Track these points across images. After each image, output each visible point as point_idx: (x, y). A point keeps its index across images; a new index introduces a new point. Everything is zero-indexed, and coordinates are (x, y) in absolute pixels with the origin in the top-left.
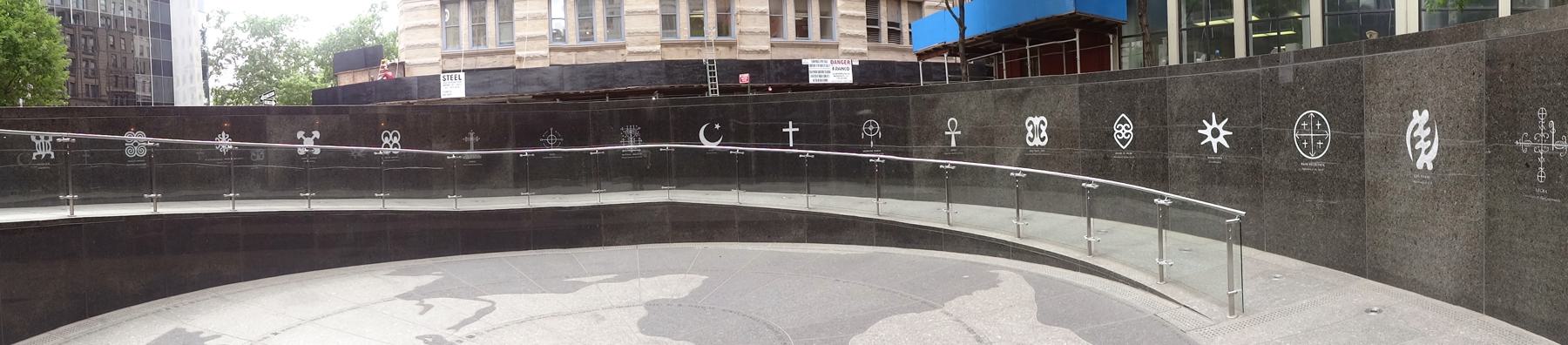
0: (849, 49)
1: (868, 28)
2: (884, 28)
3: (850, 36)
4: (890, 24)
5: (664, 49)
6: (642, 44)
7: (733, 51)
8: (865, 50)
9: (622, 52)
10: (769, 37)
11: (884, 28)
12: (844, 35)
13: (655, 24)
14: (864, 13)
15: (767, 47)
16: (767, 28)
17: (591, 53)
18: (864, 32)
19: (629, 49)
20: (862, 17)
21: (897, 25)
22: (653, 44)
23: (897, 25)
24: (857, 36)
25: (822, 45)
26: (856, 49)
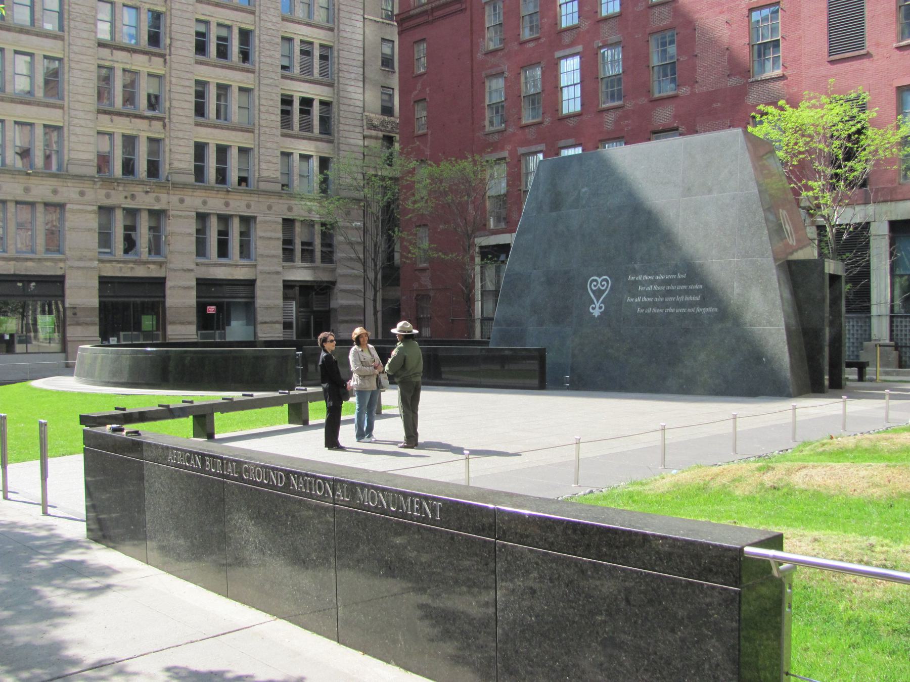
0: (267, 268)
1: (284, 249)
2: (298, 248)
3: (268, 256)
4: (303, 244)
5: (101, 265)
6: (81, 259)
7: (163, 269)
8: (280, 269)
9: (61, 265)
10: (195, 257)
11: (298, 248)
12: (262, 256)
13: (93, 240)
14: (280, 235)
15: (193, 266)
16: (193, 248)
17: (30, 264)
18: (280, 252)
19: (69, 263)
20: (278, 239)
21: (310, 244)
22: (91, 260)
23: (310, 244)
24: (274, 256)
25: (241, 265)
26: (273, 269)
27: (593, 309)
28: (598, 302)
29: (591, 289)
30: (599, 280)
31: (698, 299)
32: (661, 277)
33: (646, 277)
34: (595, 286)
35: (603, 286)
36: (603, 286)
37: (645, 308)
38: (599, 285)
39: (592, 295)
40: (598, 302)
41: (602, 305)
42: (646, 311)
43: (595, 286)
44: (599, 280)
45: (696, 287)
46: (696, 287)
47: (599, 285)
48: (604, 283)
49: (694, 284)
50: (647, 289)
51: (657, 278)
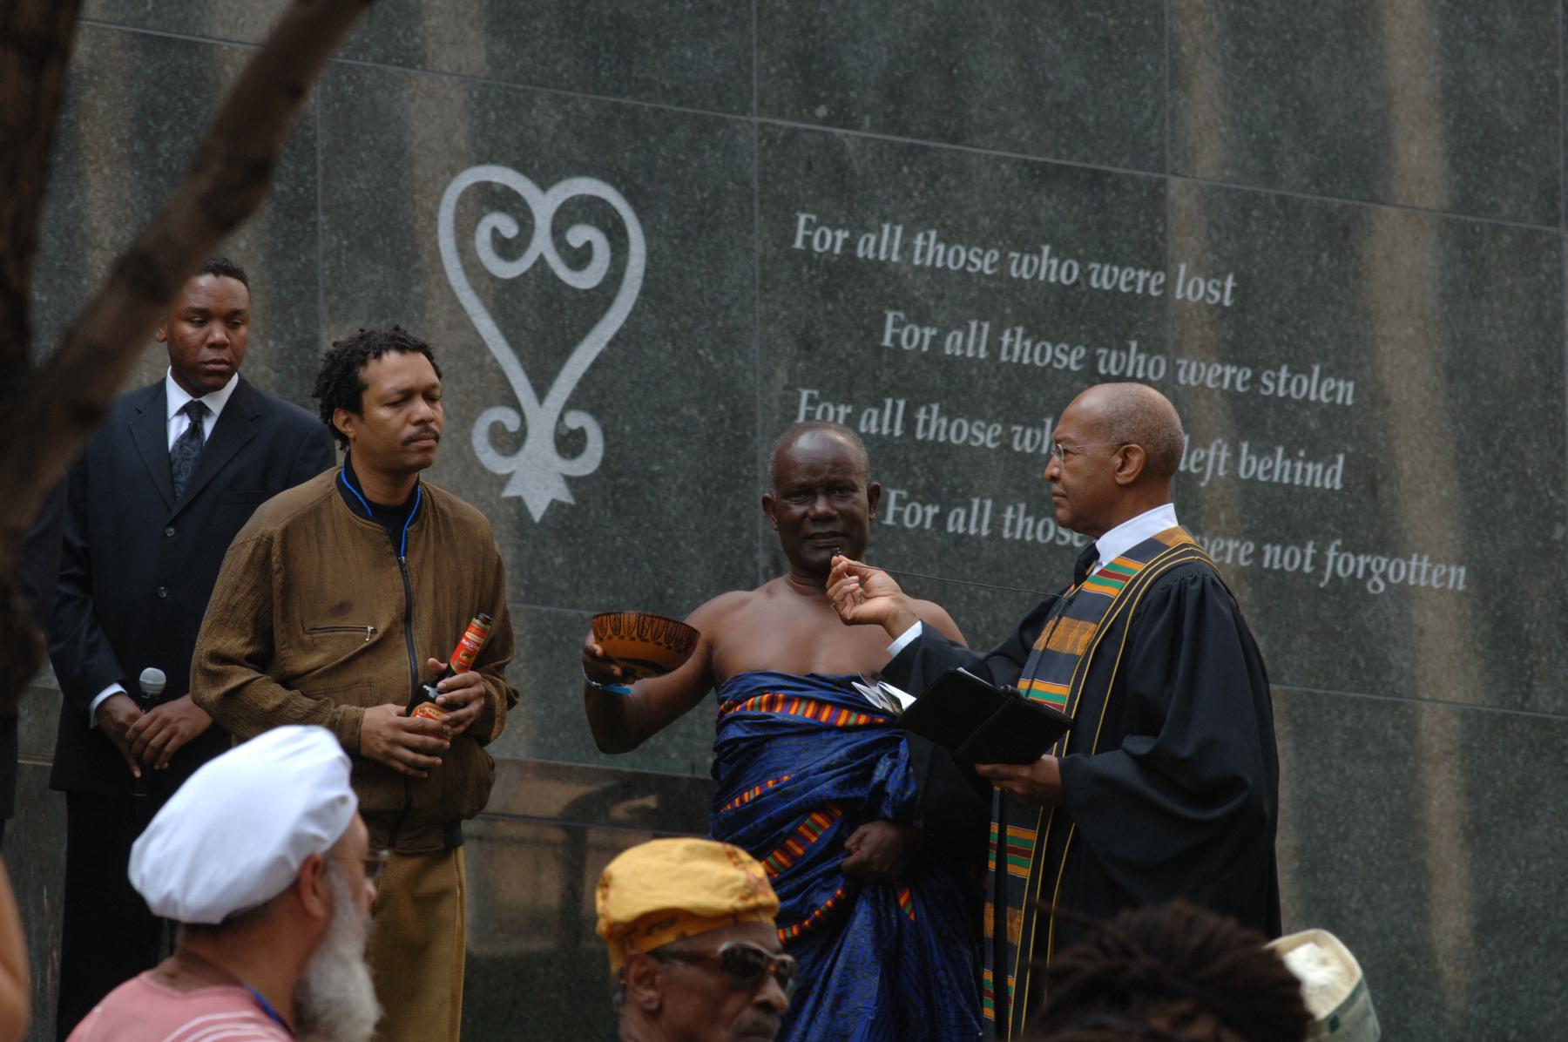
27: (511, 442)
28: (541, 392)
29: (473, 269)
30: (544, 205)
31: (1327, 476)
32: (1049, 267)
33: (931, 250)
34: (507, 249)
35: (579, 258)
36: (579, 258)
37: (948, 495)
38: (542, 243)
39: (486, 326)
40: (541, 392)
41: (576, 420)
42: (956, 523)
43: (507, 249)
44: (544, 205)
45: (1315, 387)
46: (1315, 387)
47: (542, 243)
48: (579, 235)
49: (1300, 367)
50: (953, 345)
51: (1020, 268)
